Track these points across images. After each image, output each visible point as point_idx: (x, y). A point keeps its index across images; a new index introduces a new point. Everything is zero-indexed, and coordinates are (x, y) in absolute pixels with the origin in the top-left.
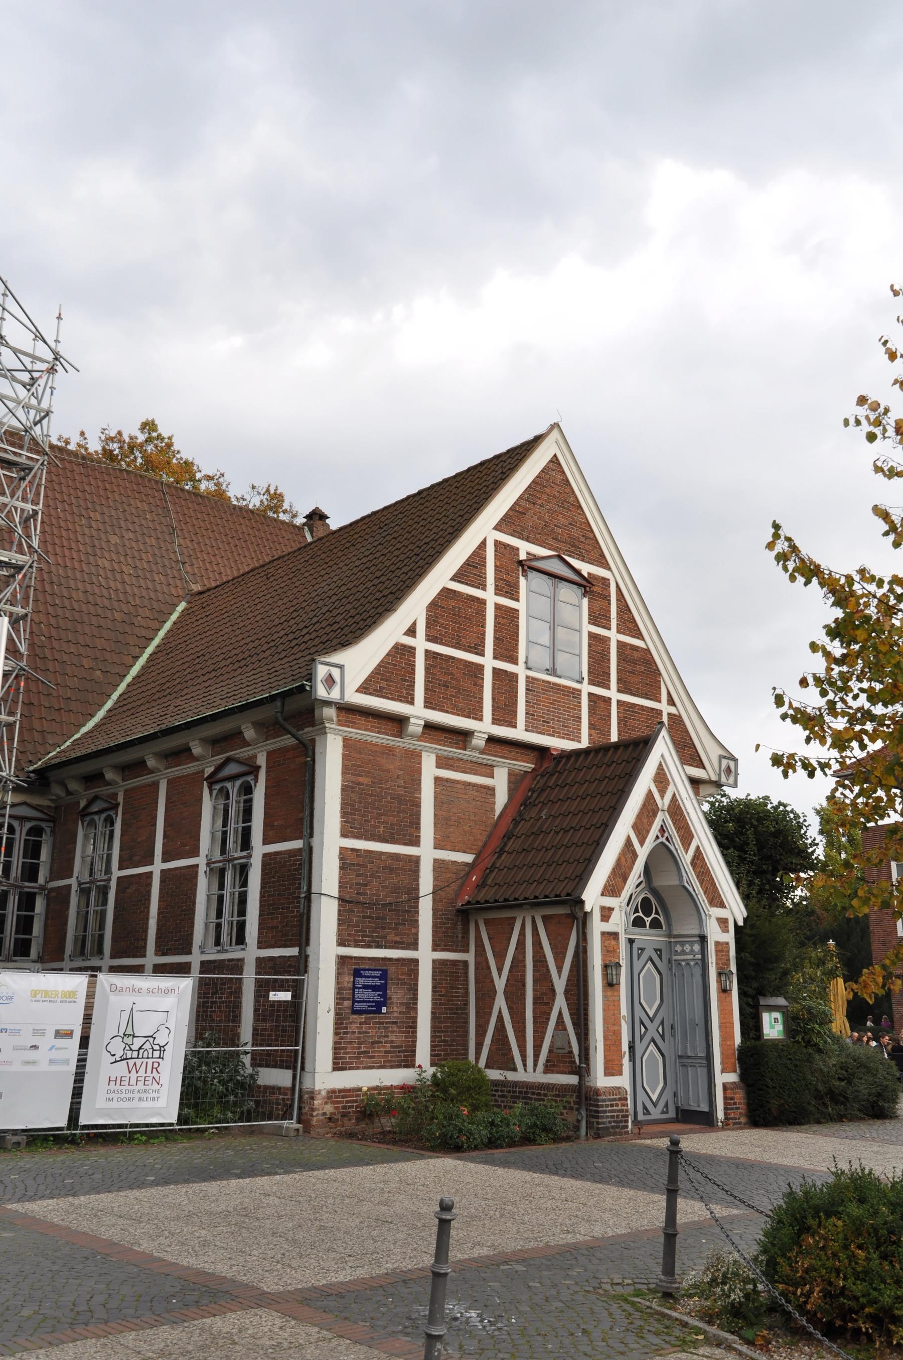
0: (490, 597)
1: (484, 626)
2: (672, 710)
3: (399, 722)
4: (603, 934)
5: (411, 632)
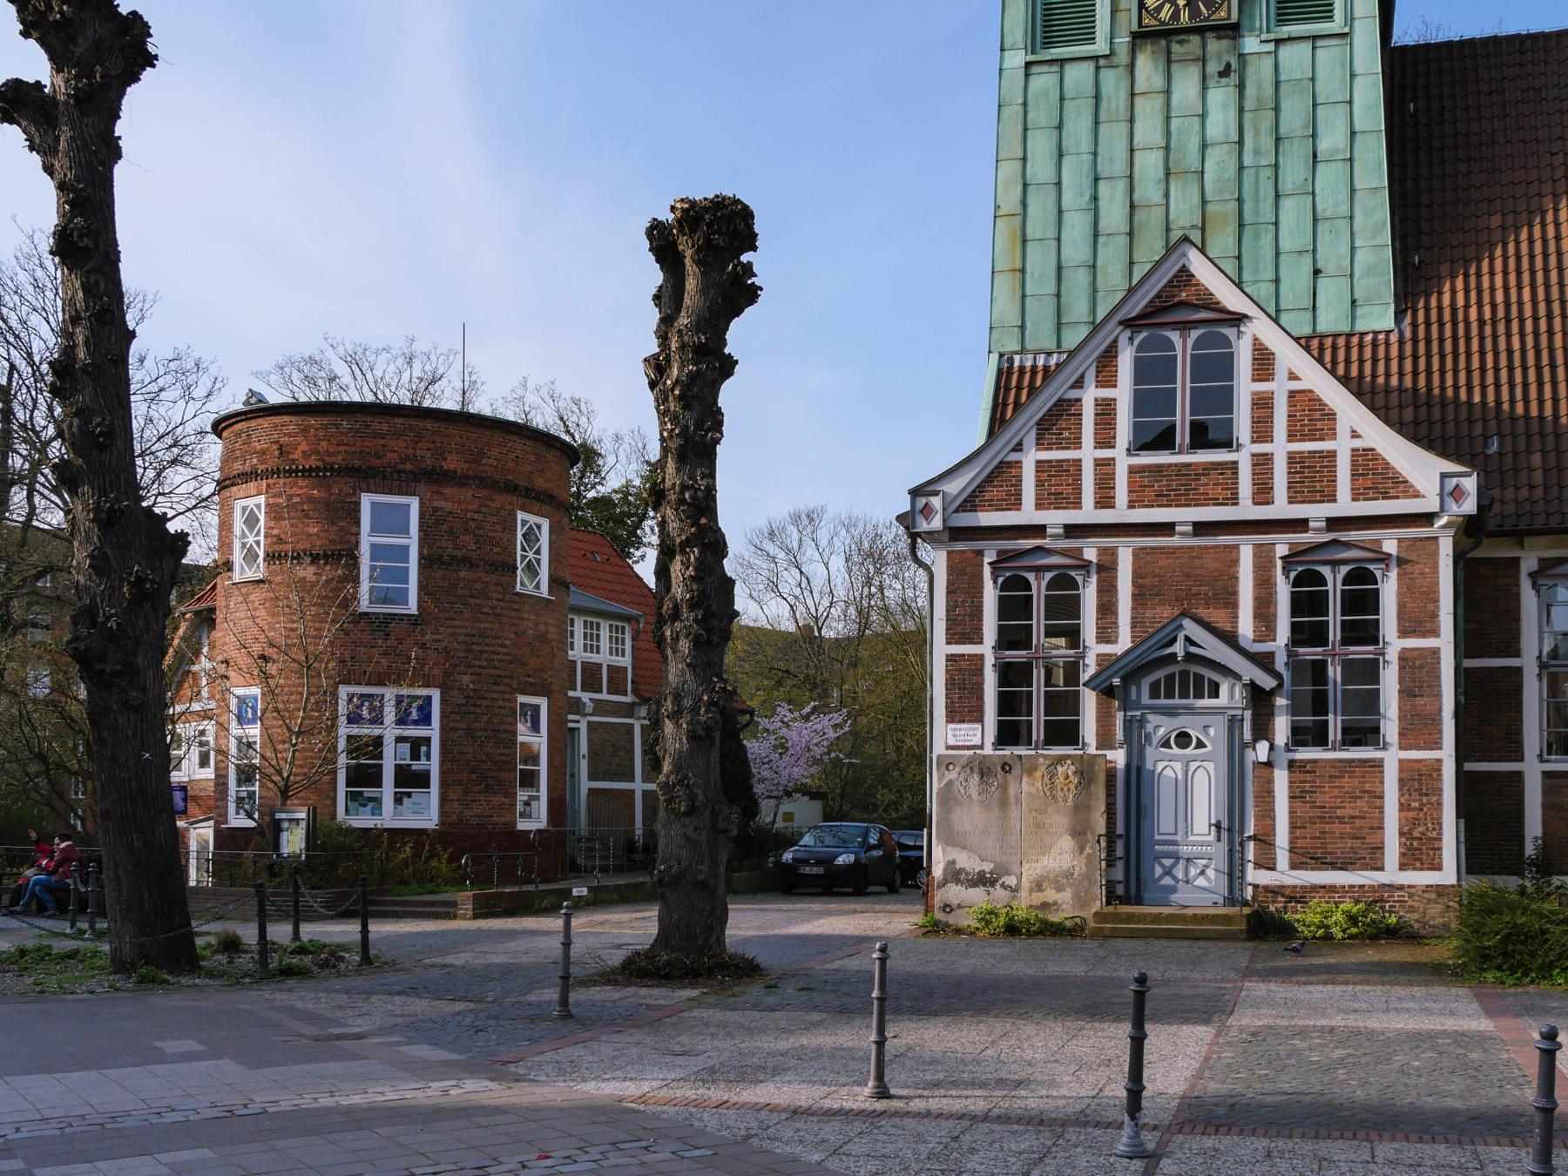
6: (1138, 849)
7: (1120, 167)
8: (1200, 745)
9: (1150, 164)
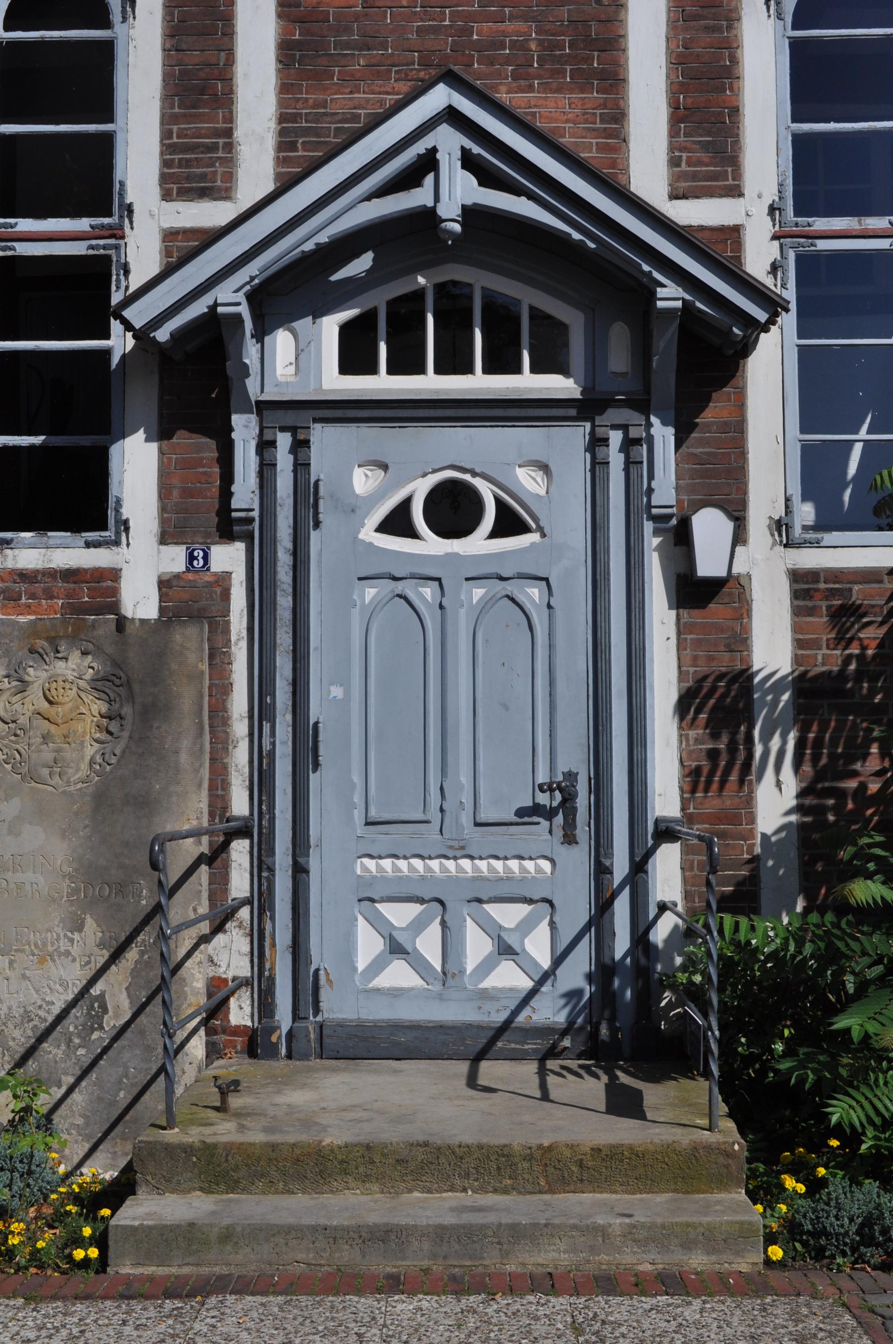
6: (299, 871)
8: (509, 523)
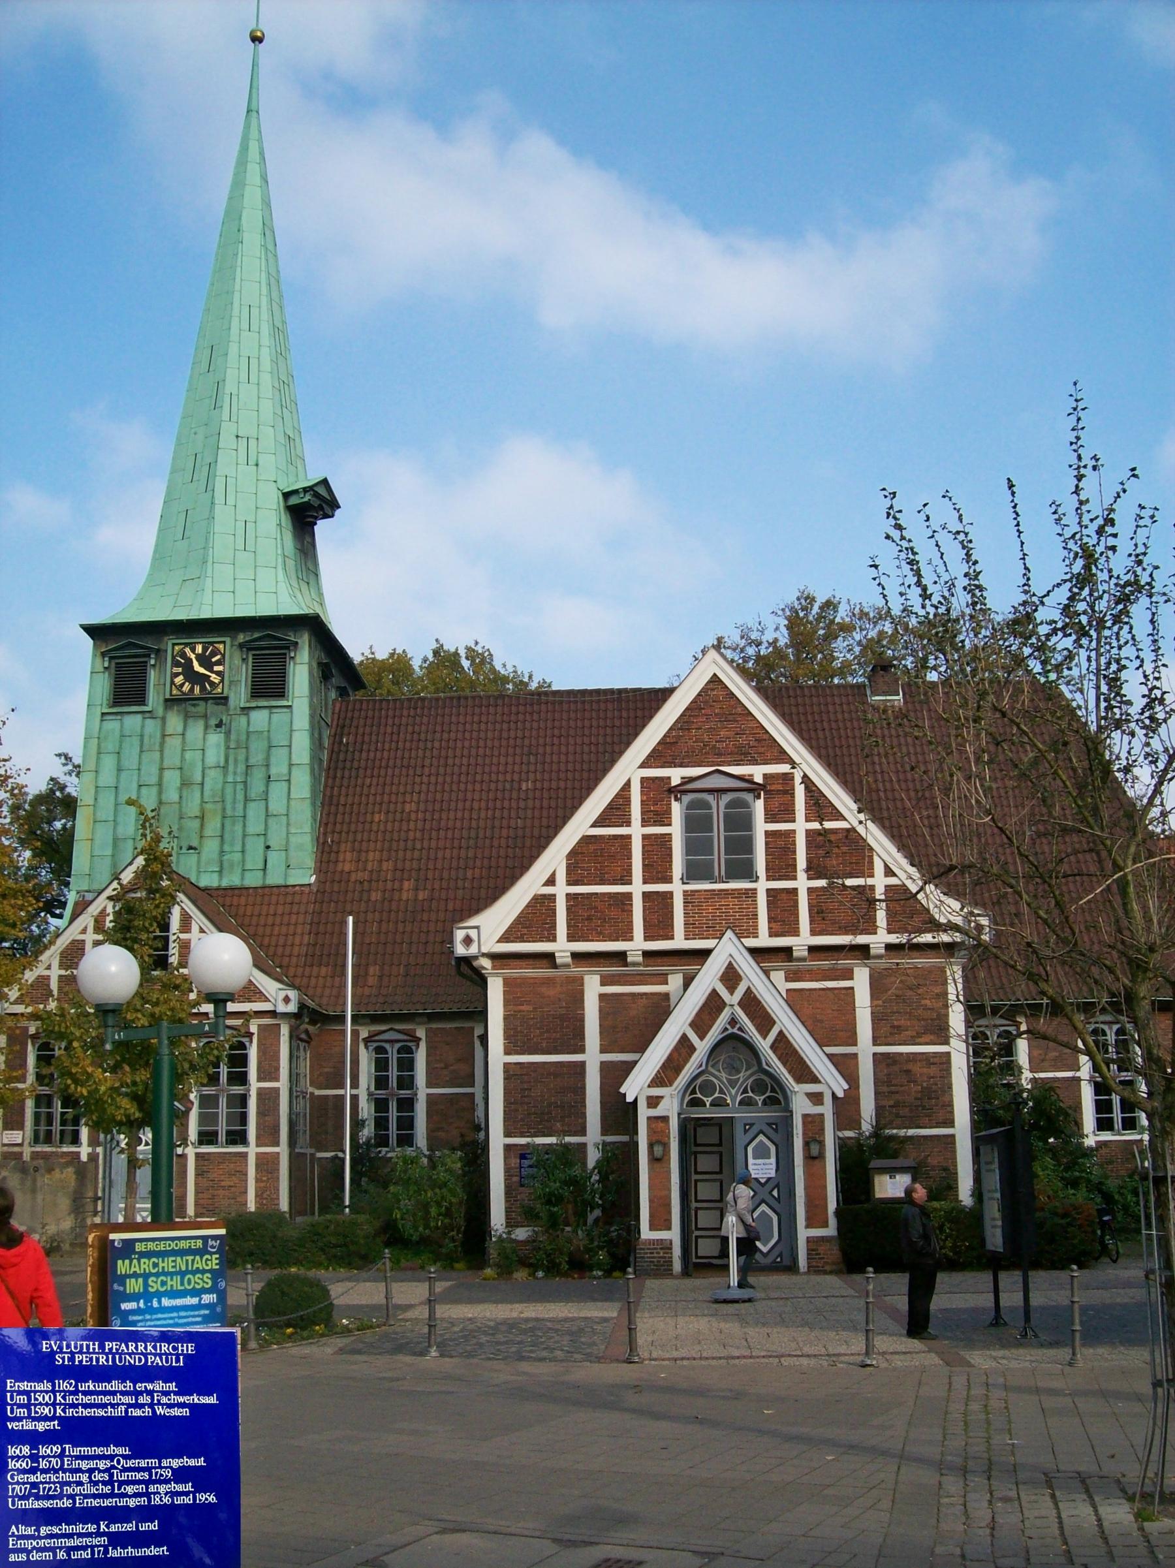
0: (636, 831)
1: (630, 857)
2: (893, 881)
3: (549, 957)
4: (649, 1118)
5: (551, 881)
7: (154, 780)
9: (172, 779)
